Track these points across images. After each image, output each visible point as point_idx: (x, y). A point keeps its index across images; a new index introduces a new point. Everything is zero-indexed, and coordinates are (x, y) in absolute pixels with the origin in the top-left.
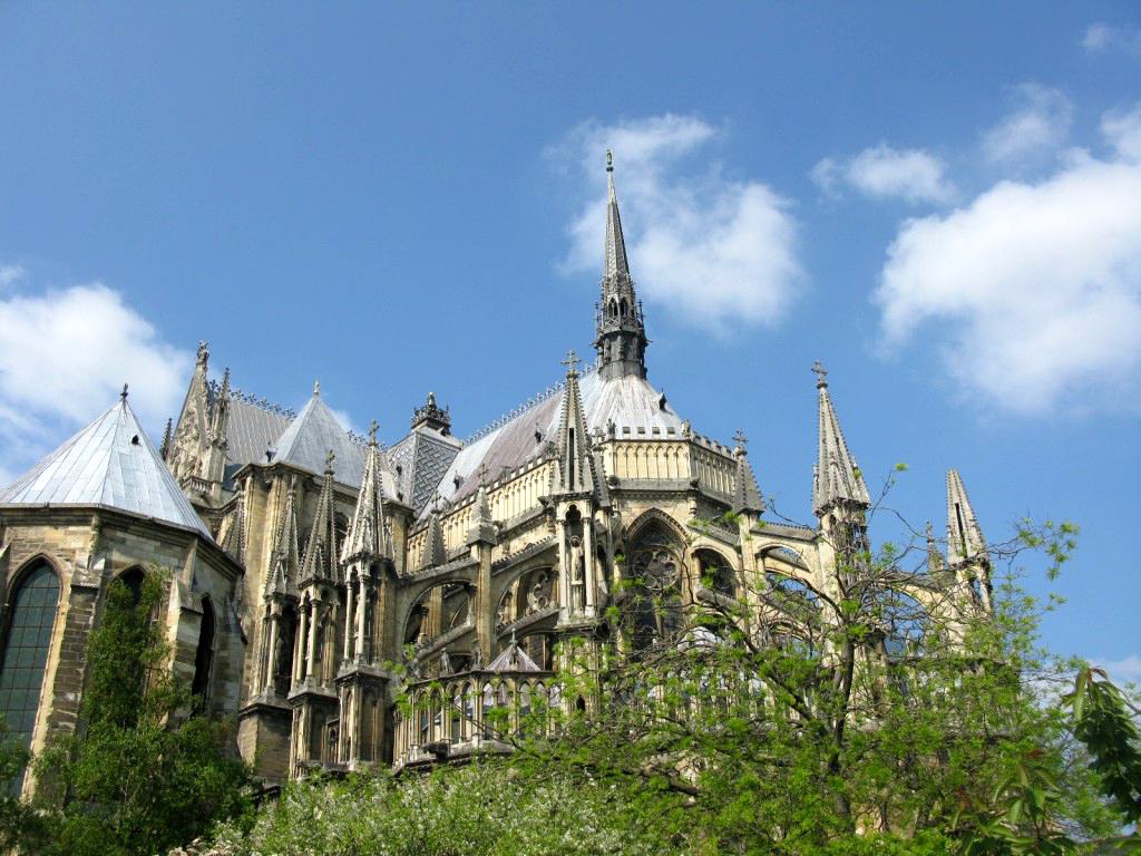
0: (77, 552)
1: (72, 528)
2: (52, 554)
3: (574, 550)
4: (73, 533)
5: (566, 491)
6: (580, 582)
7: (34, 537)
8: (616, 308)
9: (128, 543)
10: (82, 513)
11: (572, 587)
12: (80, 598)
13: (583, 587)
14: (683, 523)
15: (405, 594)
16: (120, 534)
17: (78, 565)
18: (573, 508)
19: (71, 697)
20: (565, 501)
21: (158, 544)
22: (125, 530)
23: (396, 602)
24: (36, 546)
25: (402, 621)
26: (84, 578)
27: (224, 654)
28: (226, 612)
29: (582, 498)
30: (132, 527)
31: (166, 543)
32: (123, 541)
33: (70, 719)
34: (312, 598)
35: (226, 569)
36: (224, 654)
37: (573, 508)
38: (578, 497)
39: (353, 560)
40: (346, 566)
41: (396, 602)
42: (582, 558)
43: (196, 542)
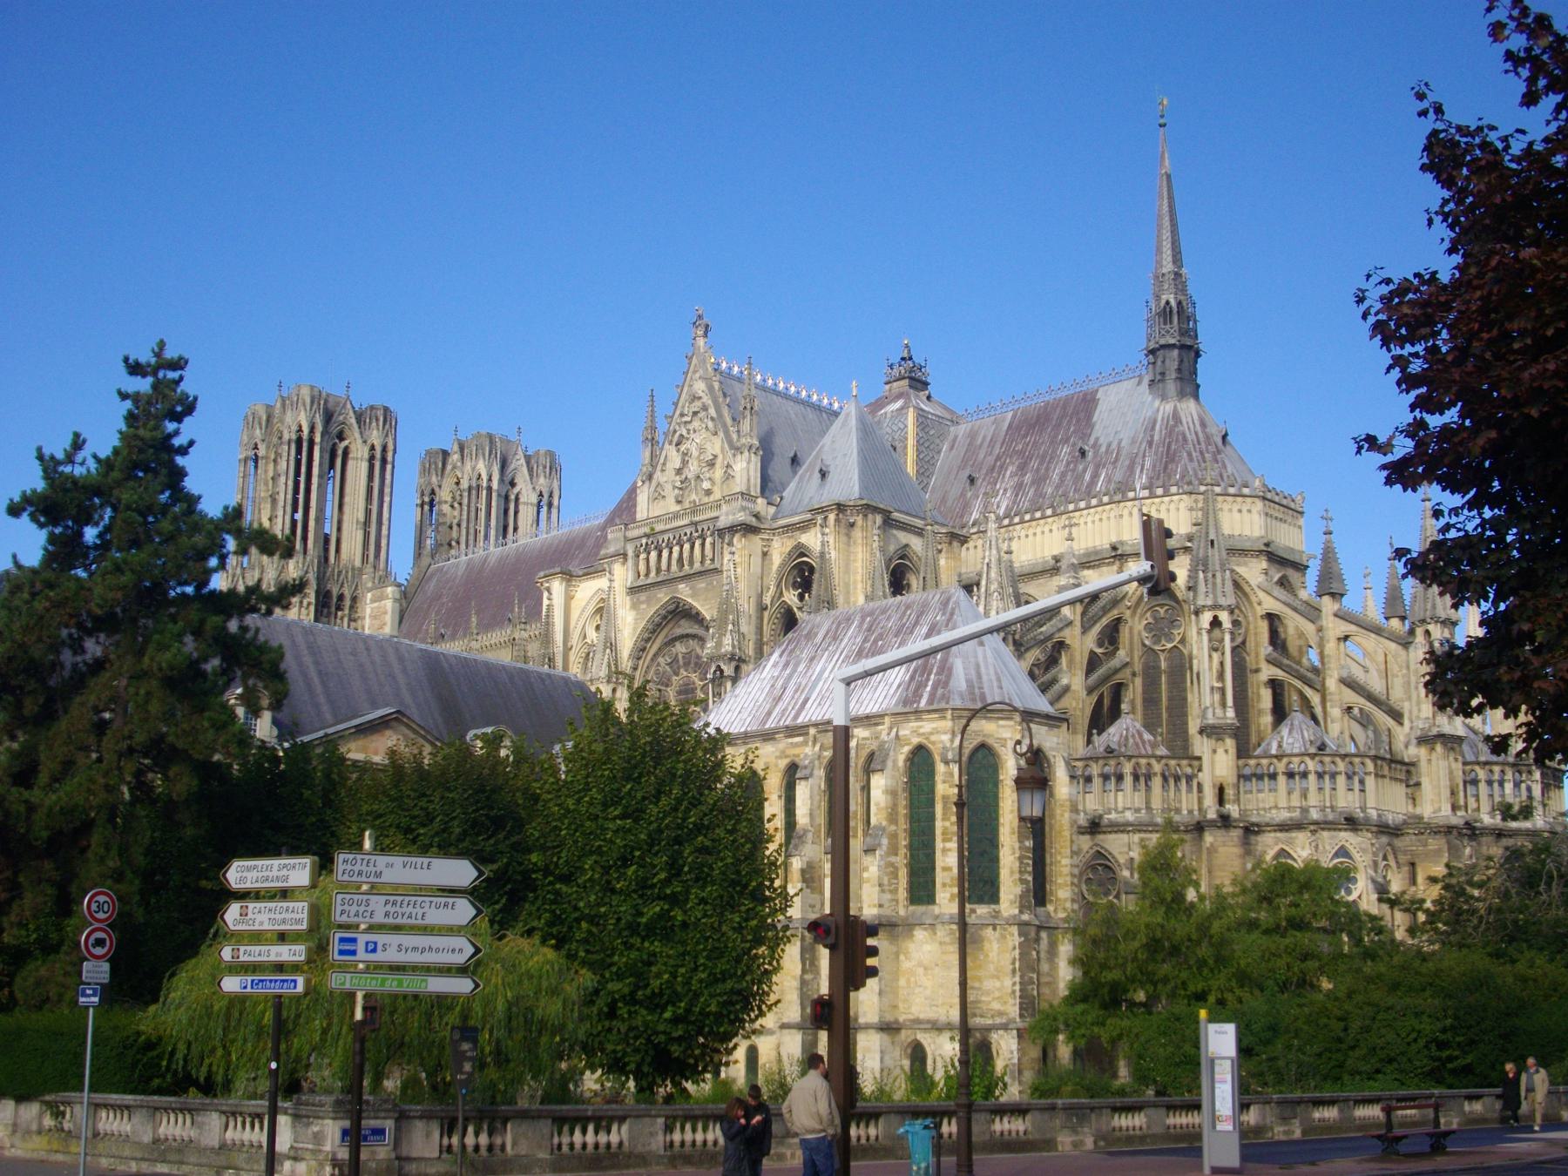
1: (1001, 722)
2: (990, 741)
3: (1215, 656)
4: (1003, 726)
5: (1209, 602)
6: (1220, 685)
8: (1171, 312)
11: (1212, 688)
13: (1222, 691)
14: (1254, 583)
18: (1215, 617)
19: (1027, 844)
33: (1029, 858)
37: (1215, 617)
38: (1220, 607)
42: (1222, 664)
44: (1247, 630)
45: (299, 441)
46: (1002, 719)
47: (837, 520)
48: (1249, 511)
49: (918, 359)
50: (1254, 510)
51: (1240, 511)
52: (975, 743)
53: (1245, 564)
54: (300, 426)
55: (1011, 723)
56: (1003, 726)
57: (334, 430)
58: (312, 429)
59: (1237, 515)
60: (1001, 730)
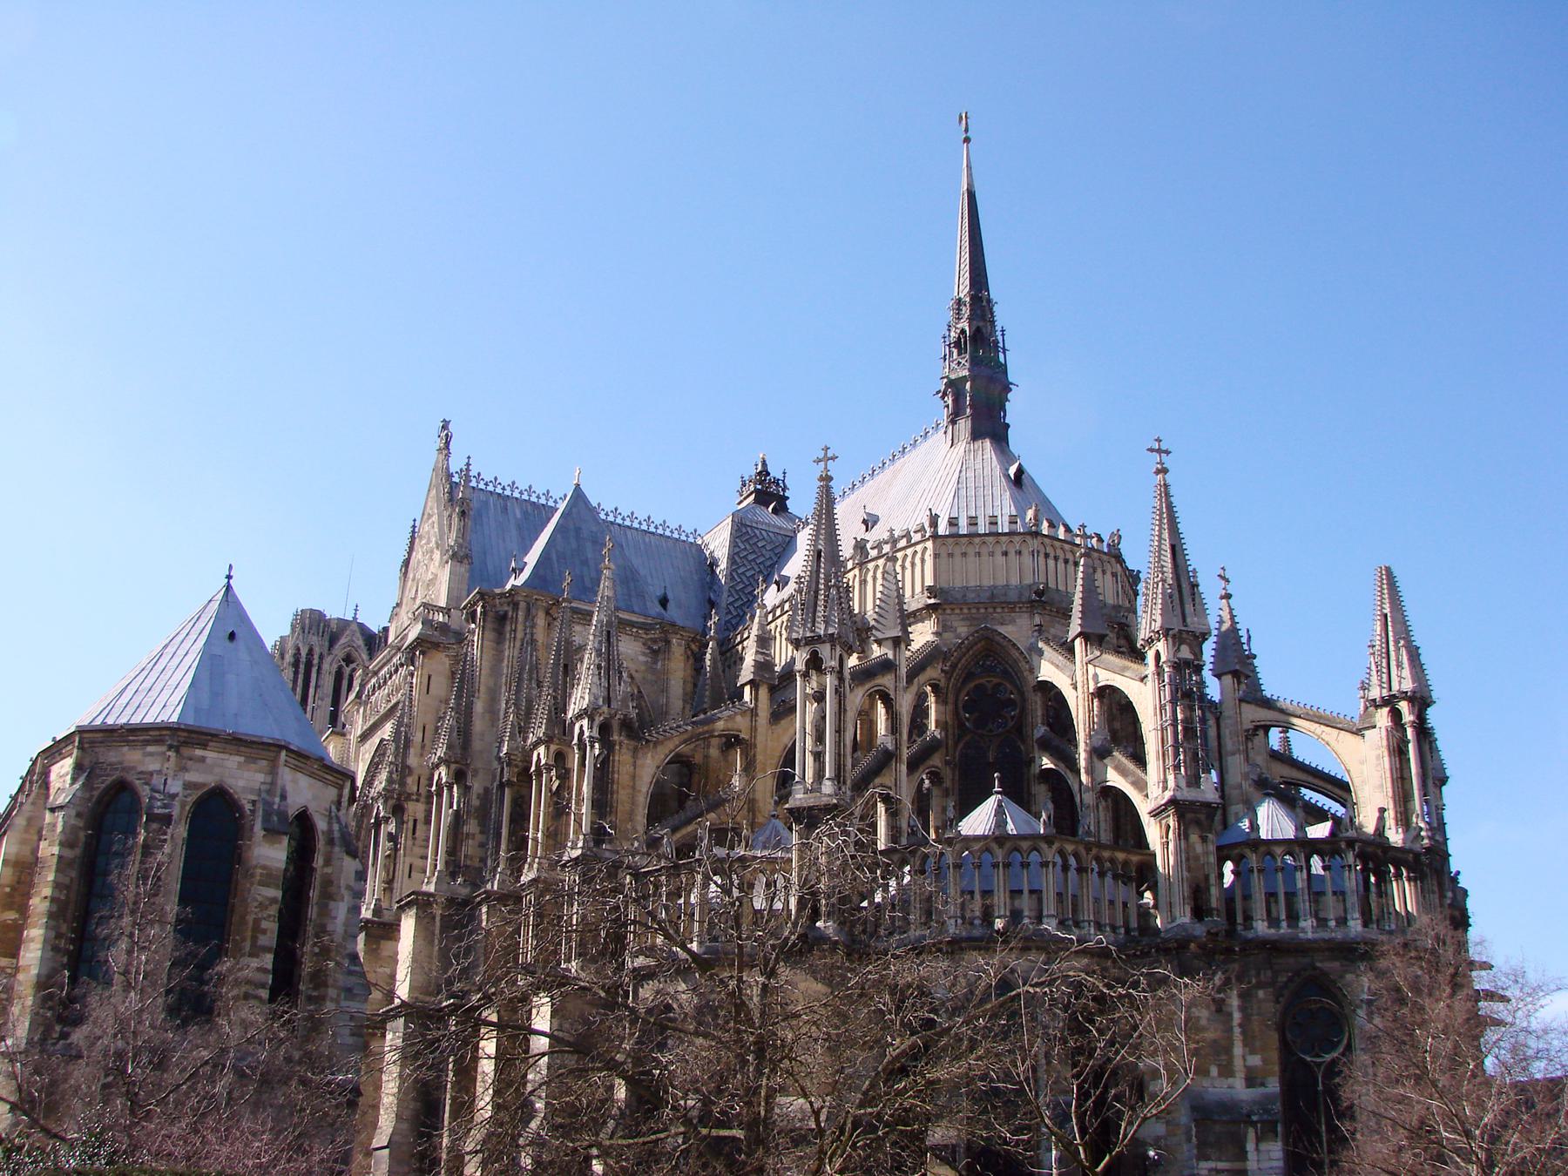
0: (155, 776)
1: (150, 749)
2: (131, 777)
4: (151, 754)
7: (114, 760)
9: (208, 761)
10: (158, 733)
12: (155, 826)
15: (649, 755)
16: (199, 752)
17: (154, 790)
20: (806, 644)
21: (242, 759)
22: (204, 746)
23: (635, 765)
24: (117, 769)
25: (644, 790)
26: (159, 803)
27: (328, 870)
28: (330, 823)
29: (824, 642)
30: (211, 744)
31: (251, 760)
32: (203, 759)
34: (543, 762)
35: (330, 778)
36: (328, 870)
39: (579, 717)
40: (573, 724)
41: (635, 765)
43: (283, 753)
44: (1023, 710)
45: (296, 664)
46: (147, 743)
47: (484, 613)
48: (1019, 553)
49: (775, 472)
50: (1025, 552)
51: (1005, 554)
52: (110, 779)
53: (1013, 622)
54: (298, 649)
55: (164, 748)
56: (151, 754)
57: (339, 652)
58: (310, 652)
59: (1000, 559)
60: (148, 759)
